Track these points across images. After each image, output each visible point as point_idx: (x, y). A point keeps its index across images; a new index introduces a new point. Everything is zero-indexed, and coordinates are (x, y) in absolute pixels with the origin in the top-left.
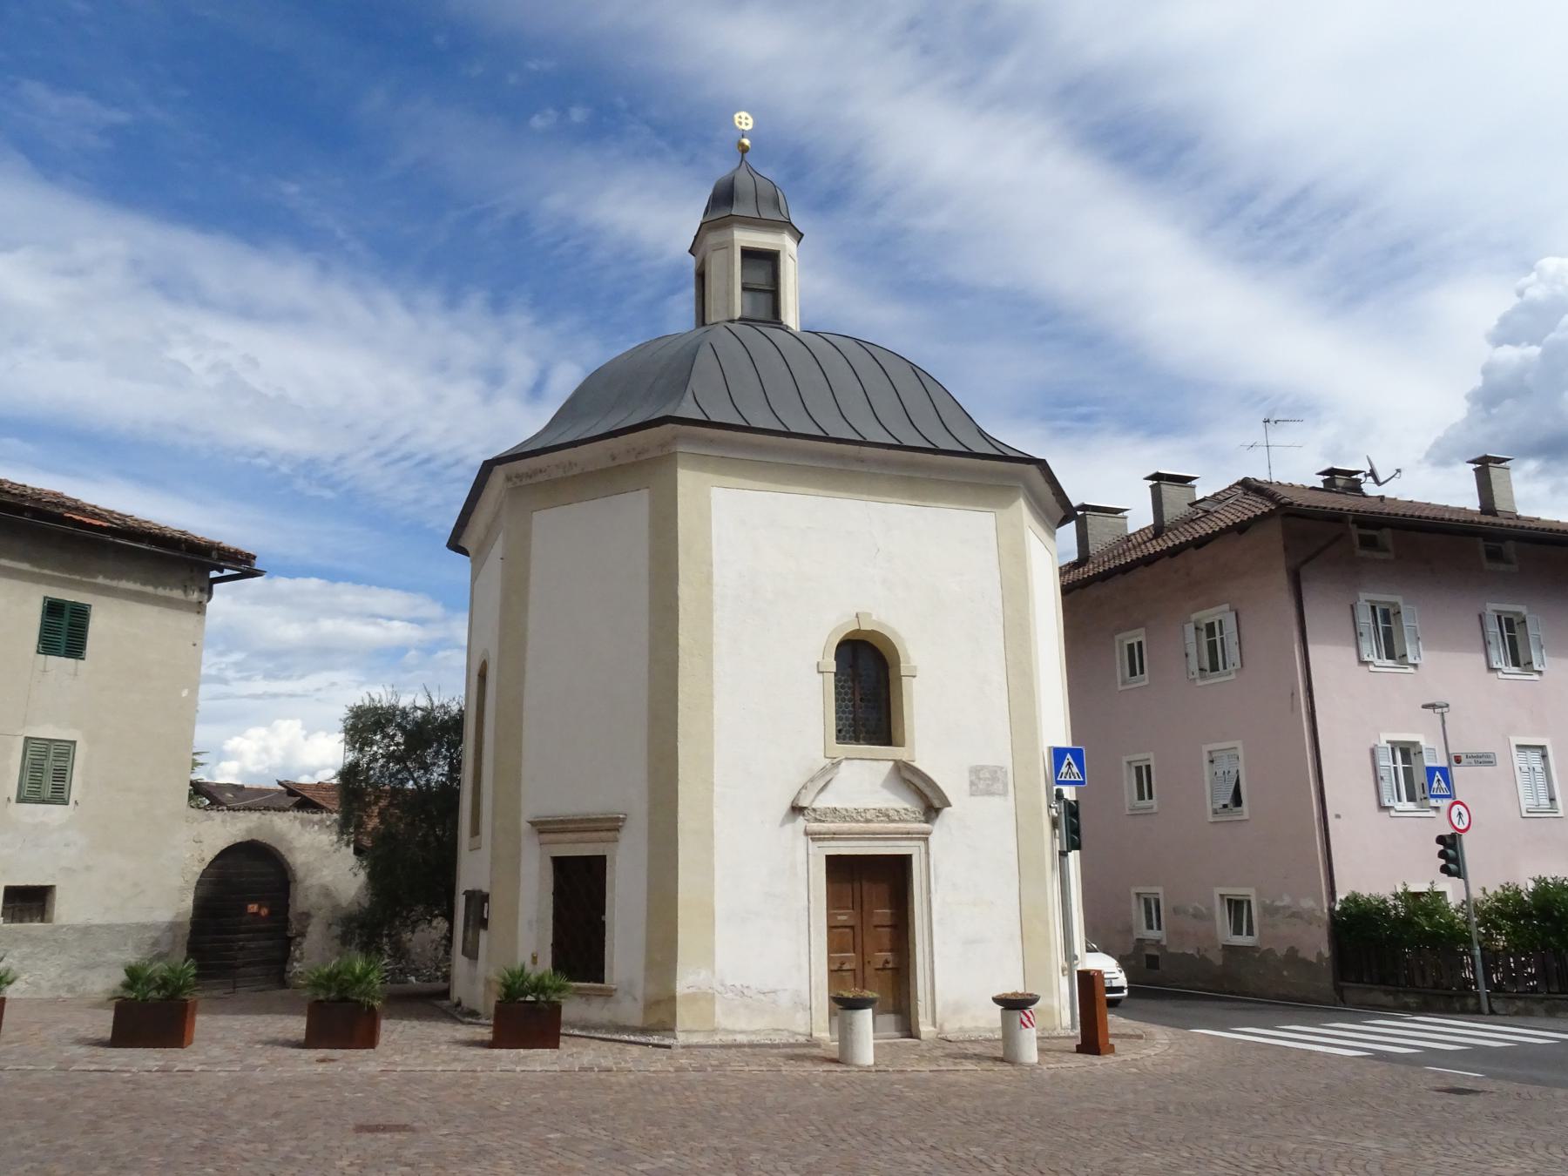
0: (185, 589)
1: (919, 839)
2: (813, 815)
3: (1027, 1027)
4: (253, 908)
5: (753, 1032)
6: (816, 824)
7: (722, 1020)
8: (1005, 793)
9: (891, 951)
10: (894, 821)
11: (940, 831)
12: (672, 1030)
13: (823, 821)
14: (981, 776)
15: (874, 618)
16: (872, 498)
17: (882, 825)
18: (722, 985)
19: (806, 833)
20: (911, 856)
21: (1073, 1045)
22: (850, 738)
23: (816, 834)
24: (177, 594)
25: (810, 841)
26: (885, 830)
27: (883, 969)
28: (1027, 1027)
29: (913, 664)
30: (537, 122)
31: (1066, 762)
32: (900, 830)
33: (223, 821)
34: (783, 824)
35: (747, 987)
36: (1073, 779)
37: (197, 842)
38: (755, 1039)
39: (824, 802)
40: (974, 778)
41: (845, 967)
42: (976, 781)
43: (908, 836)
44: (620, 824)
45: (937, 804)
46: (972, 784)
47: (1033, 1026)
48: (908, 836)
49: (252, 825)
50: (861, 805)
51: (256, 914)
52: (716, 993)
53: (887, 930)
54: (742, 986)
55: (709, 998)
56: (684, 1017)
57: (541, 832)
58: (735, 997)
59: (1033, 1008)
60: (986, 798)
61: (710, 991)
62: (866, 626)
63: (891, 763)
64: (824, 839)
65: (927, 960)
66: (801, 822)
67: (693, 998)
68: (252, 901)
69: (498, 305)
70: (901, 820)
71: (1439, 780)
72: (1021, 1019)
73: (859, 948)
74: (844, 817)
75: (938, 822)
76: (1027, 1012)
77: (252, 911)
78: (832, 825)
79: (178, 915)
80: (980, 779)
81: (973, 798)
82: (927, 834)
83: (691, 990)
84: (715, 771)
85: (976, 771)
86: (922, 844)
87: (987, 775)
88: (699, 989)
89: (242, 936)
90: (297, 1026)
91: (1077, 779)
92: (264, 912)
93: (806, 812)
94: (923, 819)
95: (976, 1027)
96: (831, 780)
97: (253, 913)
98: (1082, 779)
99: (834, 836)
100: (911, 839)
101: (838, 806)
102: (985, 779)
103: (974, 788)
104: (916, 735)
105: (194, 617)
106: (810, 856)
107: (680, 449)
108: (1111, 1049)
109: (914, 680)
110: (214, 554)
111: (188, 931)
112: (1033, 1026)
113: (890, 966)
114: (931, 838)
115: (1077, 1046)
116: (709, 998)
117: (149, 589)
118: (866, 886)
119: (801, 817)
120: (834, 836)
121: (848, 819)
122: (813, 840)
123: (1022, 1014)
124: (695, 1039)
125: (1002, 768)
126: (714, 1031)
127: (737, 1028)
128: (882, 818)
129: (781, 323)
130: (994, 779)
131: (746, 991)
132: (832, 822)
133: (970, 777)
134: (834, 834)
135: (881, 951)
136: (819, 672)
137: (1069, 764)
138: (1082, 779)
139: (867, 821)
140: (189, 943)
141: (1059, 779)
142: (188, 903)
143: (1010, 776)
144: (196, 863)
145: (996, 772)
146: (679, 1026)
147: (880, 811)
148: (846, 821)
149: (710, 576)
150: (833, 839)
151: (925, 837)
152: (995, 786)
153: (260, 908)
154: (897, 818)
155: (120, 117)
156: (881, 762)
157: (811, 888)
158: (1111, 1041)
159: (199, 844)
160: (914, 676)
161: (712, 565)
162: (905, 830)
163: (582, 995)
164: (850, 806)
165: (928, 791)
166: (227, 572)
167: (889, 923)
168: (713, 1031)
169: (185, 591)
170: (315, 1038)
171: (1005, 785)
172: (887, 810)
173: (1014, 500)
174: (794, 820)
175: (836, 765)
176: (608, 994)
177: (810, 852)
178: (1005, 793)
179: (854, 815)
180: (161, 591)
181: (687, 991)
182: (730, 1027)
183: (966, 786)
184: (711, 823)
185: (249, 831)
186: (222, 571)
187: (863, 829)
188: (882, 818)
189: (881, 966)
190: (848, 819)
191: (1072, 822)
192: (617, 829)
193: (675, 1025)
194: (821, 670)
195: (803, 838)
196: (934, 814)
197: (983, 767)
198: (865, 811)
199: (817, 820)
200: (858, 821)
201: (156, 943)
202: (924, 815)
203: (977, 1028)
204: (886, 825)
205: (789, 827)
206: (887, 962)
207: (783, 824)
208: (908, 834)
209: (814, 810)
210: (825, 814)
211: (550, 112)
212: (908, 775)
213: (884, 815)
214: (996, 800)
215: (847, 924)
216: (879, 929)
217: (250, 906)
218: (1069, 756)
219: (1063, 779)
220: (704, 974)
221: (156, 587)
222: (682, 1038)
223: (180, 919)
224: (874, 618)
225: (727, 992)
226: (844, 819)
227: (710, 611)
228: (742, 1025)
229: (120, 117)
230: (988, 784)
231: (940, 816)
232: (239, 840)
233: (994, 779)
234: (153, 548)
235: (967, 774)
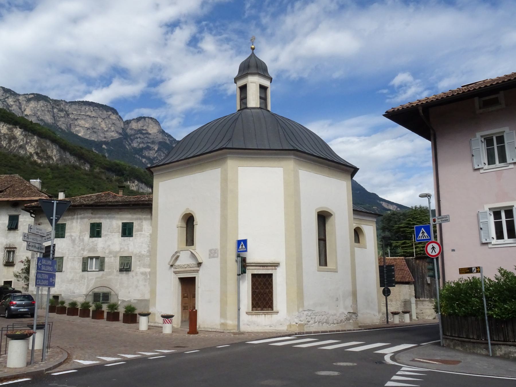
8: (217, 257)
11: (202, 269)
14: (212, 252)
26: (190, 270)
32: (192, 270)
34: (169, 269)
43: (194, 271)
46: (210, 255)
48: (194, 271)
60: (213, 259)
66: (173, 269)
80: (211, 253)
81: (210, 259)
87: (213, 252)
100: (195, 272)
119: (173, 268)
122: (175, 274)
125: (217, 249)
126: (155, 323)
130: (215, 253)
132: (178, 269)
139: (186, 268)
145: (215, 250)
150: (179, 273)
160: (197, 224)
172: (189, 264)
195: (173, 274)
198: (185, 265)
200: (184, 268)
208: (194, 271)
214: (216, 259)
233: (215, 253)
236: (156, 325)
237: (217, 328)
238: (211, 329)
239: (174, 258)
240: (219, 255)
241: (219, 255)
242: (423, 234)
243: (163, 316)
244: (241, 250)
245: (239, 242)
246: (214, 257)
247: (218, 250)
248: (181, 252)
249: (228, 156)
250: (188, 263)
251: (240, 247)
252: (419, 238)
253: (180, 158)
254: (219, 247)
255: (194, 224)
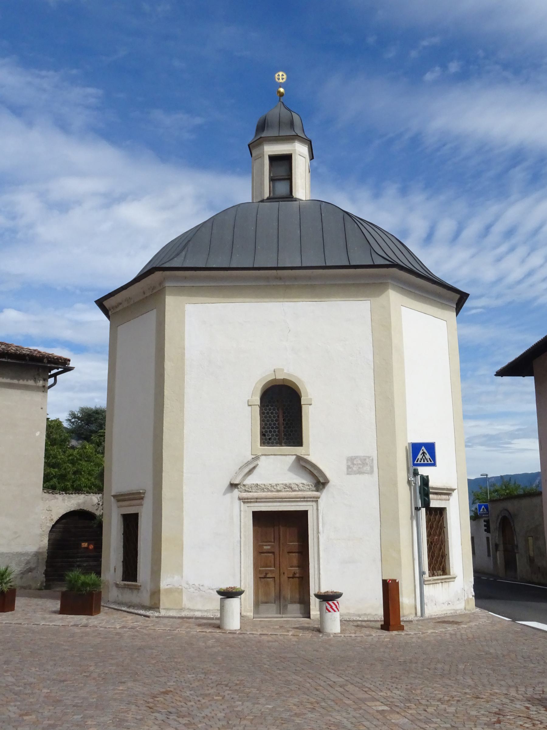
0: (35, 380)
1: (313, 501)
2: (243, 488)
3: (329, 611)
4: (85, 545)
5: (206, 611)
6: (245, 494)
7: (186, 602)
9: (299, 567)
10: (295, 491)
11: (325, 496)
12: (158, 608)
13: (250, 492)
14: (355, 462)
15: (285, 371)
16: (286, 300)
17: (287, 493)
18: (188, 584)
19: (240, 499)
20: (306, 512)
21: (379, 625)
22: (277, 443)
23: (245, 499)
24: (31, 383)
25: (242, 503)
26: (288, 496)
27: (293, 578)
28: (329, 611)
29: (309, 397)
30: (429, 77)
31: (421, 452)
32: (298, 496)
33: (63, 500)
34: (225, 494)
35: (202, 586)
36: (426, 462)
37: (48, 511)
38: (205, 614)
39: (250, 481)
40: (350, 464)
41: (268, 576)
42: (351, 466)
43: (305, 499)
44: (143, 495)
45: (322, 480)
46: (348, 467)
47: (339, 611)
48: (305, 499)
49: (80, 501)
50: (274, 482)
51: (87, 548)
52: (184, 589)
53: (297, 554)
54: (199, 585)
55: (180, 591)
56: (164, 601)
57: (118, 501)
58: (195, 591)
59: (339, 600)
60: (358, 476)
61: (180, 587)
62: (280, 377)
63: (295, 457)
64: (251, 502)
65: (317, 572)
66: (236, 493)
67: (170, 591)
68: (85, 541)
69: (404, 192)
70: (300, 490)
71: (424, 453)
72: (326, 607)
73: (277, 565)
74: (263, 489)
75: (325, 491)
76: (335, 602)
77: (84, 546)
78: (255, 494)
79: (40, 548)
80: (353, 464)
81: (348, 476)
82: (317, 498)
83: (169, 587)
84: (184, 464)
85: (351, 460)
86: (314, 504)
87: (359, 462)
88: (174, 586)
89: (78, 559)
90: (57, 605)
91: (429, 462)
92: (91, 547)
93: (239, 487)
94: (314, 489)
95: (349, 613)
96: (254, 468)
97: (84, 548)
98: (433, 462)
99: (257, 500)
100: (307, 501)
101: (259, 483)
102: (358, 464)
103: (350, 470)
104: (311, 439)
105: (41, 394)
106: (242, 513)
107: (167, 284)
108: (402, 628)
109: (310, 406)
110: (45, 361)
111: (46, 557)
112: (339, 611)
113: (297, 575)
114: (320, 501)
115: (381, 625)
116: (180, 591)
117: (15, 381)
118: (282, 529)
119: (236, 490)
120: (257, 500)
121: (265, 490)
122: (244, 502)
123: (327, 605)
124: (172, 613)
125: (369, 457)
126: (182, 609)
127: (196, 608)
128: (288, 489)
129: (293, 197)
130: (364, 464)
131: (201, 588)
132: (256, 492)
133: (347, 462)
134: (257, 499)
135: (292, 567)
136: (249, 405)
137: (424, 453)
138: (433, 462)
139: (278, 491)
140: (47, 562)
141: (415, 462)
142: (45, 542)
143: (375, 462)
144: (49, 522)
145: (365, 460)
146: (162, 606)
147: (286, 485)
148: (264, 491)
149: (183, 354)
150: (256, 502)
151: (316, 500)
152: (365, 468)
153: (88, 545)
154: (297, 489)
155: (198, 121)
156: (288, 456)
157: (242, 530)
158: (402, 623)
159: (49, 512)
161: (184, 349)
162: (301, 496)
163: (131, 589)
164: (267, 482)
165: (315, 472)
166: (60, 370)
167: (297, 551)
168: (182, 609)
169: (35, 381)
170: (64, 611)
171: (372, 467)
172: (290, 484)
173: (388, 289)
174: (232, 492)
175: (257, 458)
176: (138, 588)
177: (242, 509)
178: (372, 472)
179: (269, 488)
180: (21, 382)
181: (167, 587)
182: (192, 608)
183: (345, 469)
184: (182, 494)
185: (79, 504)
186: (58, 369)
187: (274, 496)
188: (288, 489)
189: (291, 576)
190: (265, 490)
191: (424, 489)
192: (142, 498)
193: (160, 606)
194: (250, 404)
195: (237, 502)
196: (321, 487)
197: (356, 457)
199: (246, 491)
200: (272, 491)
201: (28, 563)
202: (315, 486)
203: (349, 614)
204: (290, 493)
205: (229, 495)
206: (295, 574)
207: (225, 494)
209: (244, 485)
210: (251, 487)
211: (437, 69)
212: (304, 464)
213: (289, 487)
214: (366, 476)
215: (270, 551)
216: (291, 554)
217: (83, 544)
218: (423, 448)
219: (419, 462)
220: (176, 578)
221: (19, 380)
222: (163, 613)
223: (41, 551)
224: (285, 371)
225: (190, 588)
226: (263, 490)
227: (183, 374)
228: (199, 607)
229: (198, 121)
230: (359, 468)
231: (326, 488)
232: (72, 510)
233: (364, 464)
234: (9, 360)
235: (345, 462)
236: (183, 614)
237: (374, 613)
238: (359, 616)
239: (247, 470)
240: (375, 469)
241: (375, 469)
242: (424, 455)
243: (220, 593)
244: (422, 462)
245: (416, 448)
246: (360, 473)
247: (373, 460)
248: (263, 458)
249: (389, 281)
250: (287, 482)
251: (420, 456)
252: (417, 461)
253: (158, 263)
254: (374, 455)
255: (302, 403)
